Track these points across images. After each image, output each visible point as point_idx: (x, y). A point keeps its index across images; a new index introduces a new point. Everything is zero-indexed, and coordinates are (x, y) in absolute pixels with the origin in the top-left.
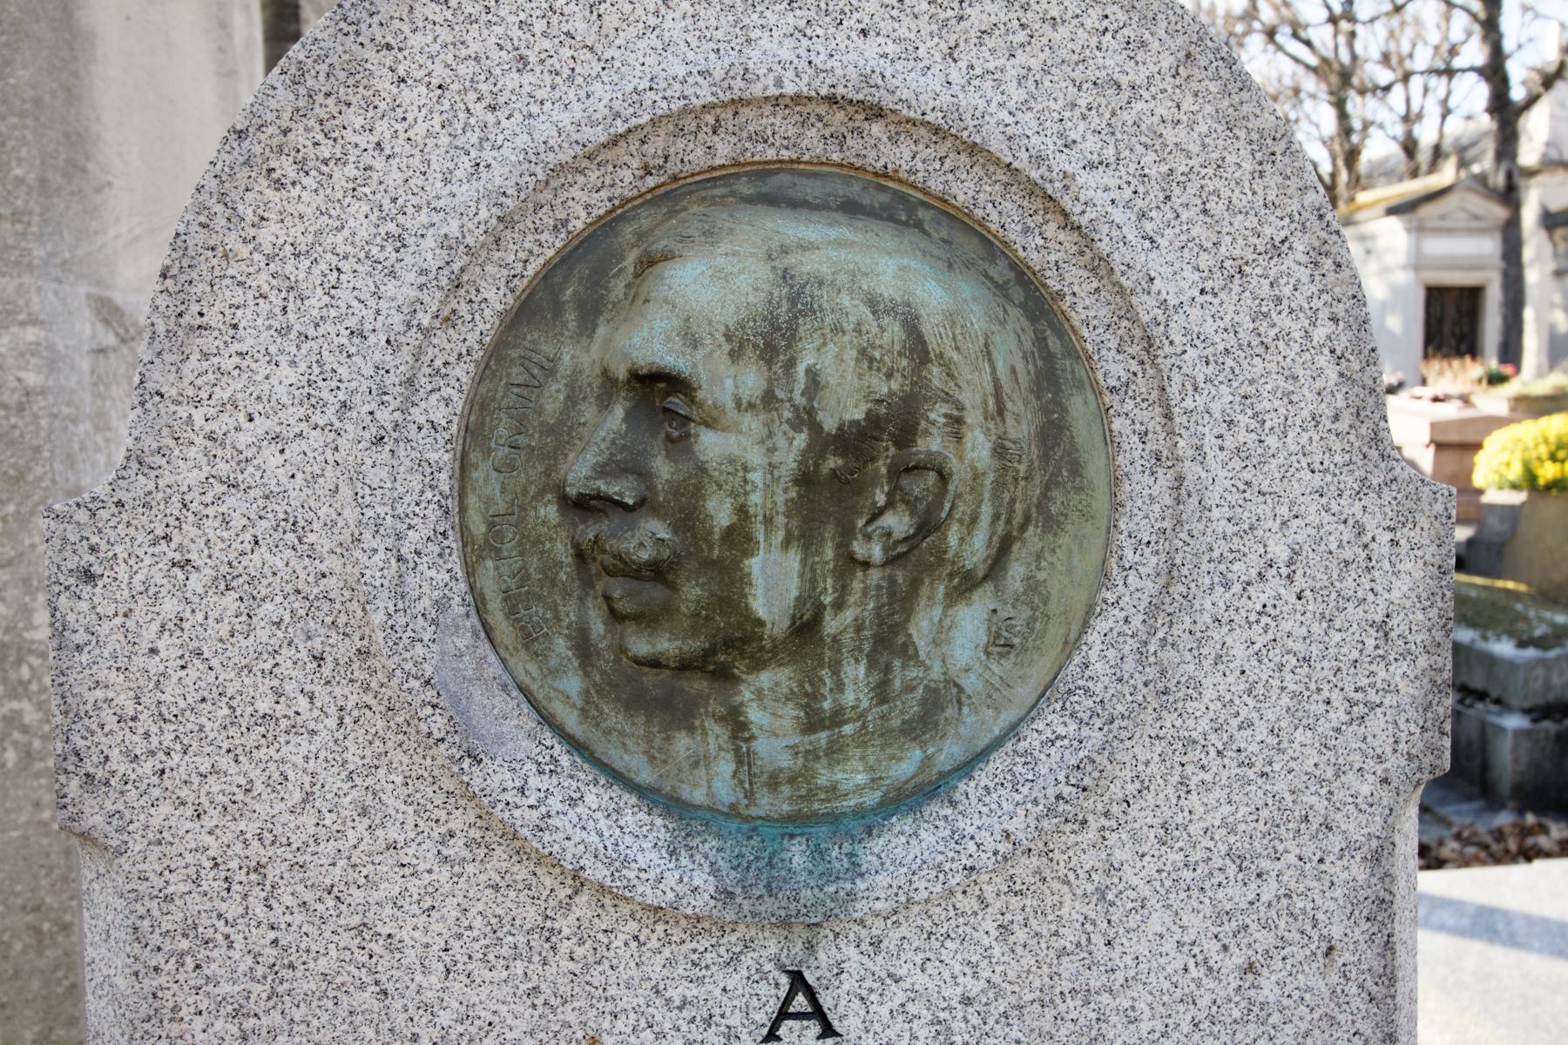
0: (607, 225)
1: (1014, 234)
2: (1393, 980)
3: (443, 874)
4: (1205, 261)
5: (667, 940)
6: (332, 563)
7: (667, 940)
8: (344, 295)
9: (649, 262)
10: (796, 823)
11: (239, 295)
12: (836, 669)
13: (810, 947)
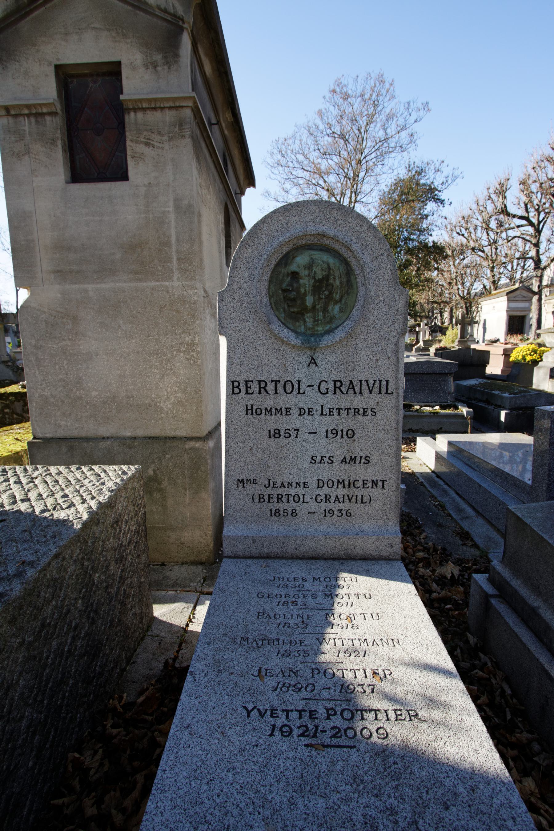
0: (288, 253)
1: (343, 253)
2: (398, 363)
3: (266, 341)
4: (371, 257)
5: (295, 351)
6: (252, 299)
7: (295, 351)
8: (254, 263)
9: (294, 258)
10: (312, 335)
11: (241, 263)
12: (318, 313)
13: (314, 353)
